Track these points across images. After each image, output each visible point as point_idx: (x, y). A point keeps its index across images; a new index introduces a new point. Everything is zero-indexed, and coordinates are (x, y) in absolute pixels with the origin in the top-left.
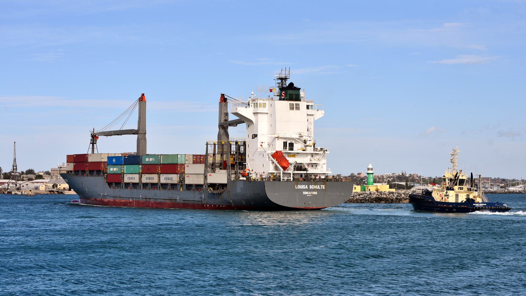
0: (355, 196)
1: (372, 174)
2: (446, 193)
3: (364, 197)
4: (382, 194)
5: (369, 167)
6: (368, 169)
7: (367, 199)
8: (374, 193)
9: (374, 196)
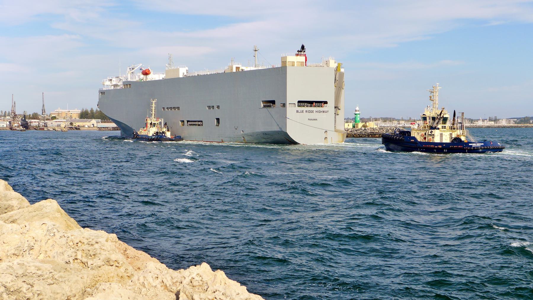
1: (359, 114)
2: (431, 132)
6: (356, 111)
9: (369, 131)
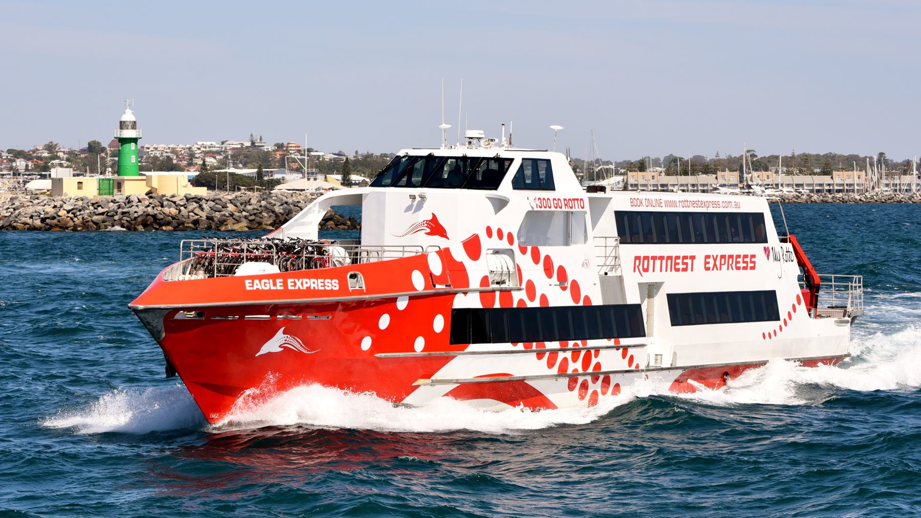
0: (80, 211)
1: (135, 140)
4: (165, 203)
6: (122, 125)
8: (140, 201)
9: (141, 210)
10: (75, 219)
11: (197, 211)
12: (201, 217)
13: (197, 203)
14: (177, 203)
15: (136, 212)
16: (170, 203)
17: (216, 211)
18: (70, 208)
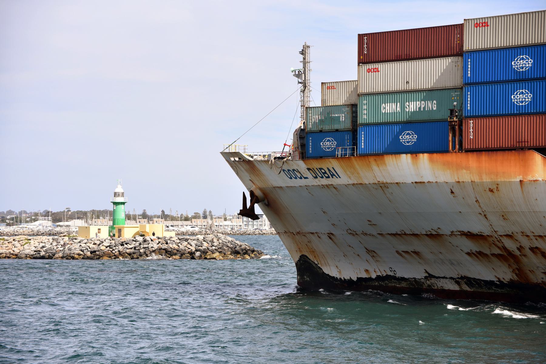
1: (123, 203)
3: (135, 248)
4: (169, 242)
5: (115, 191)
6: (116, 194)
7: (142, 251)
10: (114, 252)
11: (189, 246)
12: (192, 250)
13: (186, 241)
14: (176, 241)
15: (152, 247)
16: (171, 241)
17: (199, 246)
18: (108, 245)
